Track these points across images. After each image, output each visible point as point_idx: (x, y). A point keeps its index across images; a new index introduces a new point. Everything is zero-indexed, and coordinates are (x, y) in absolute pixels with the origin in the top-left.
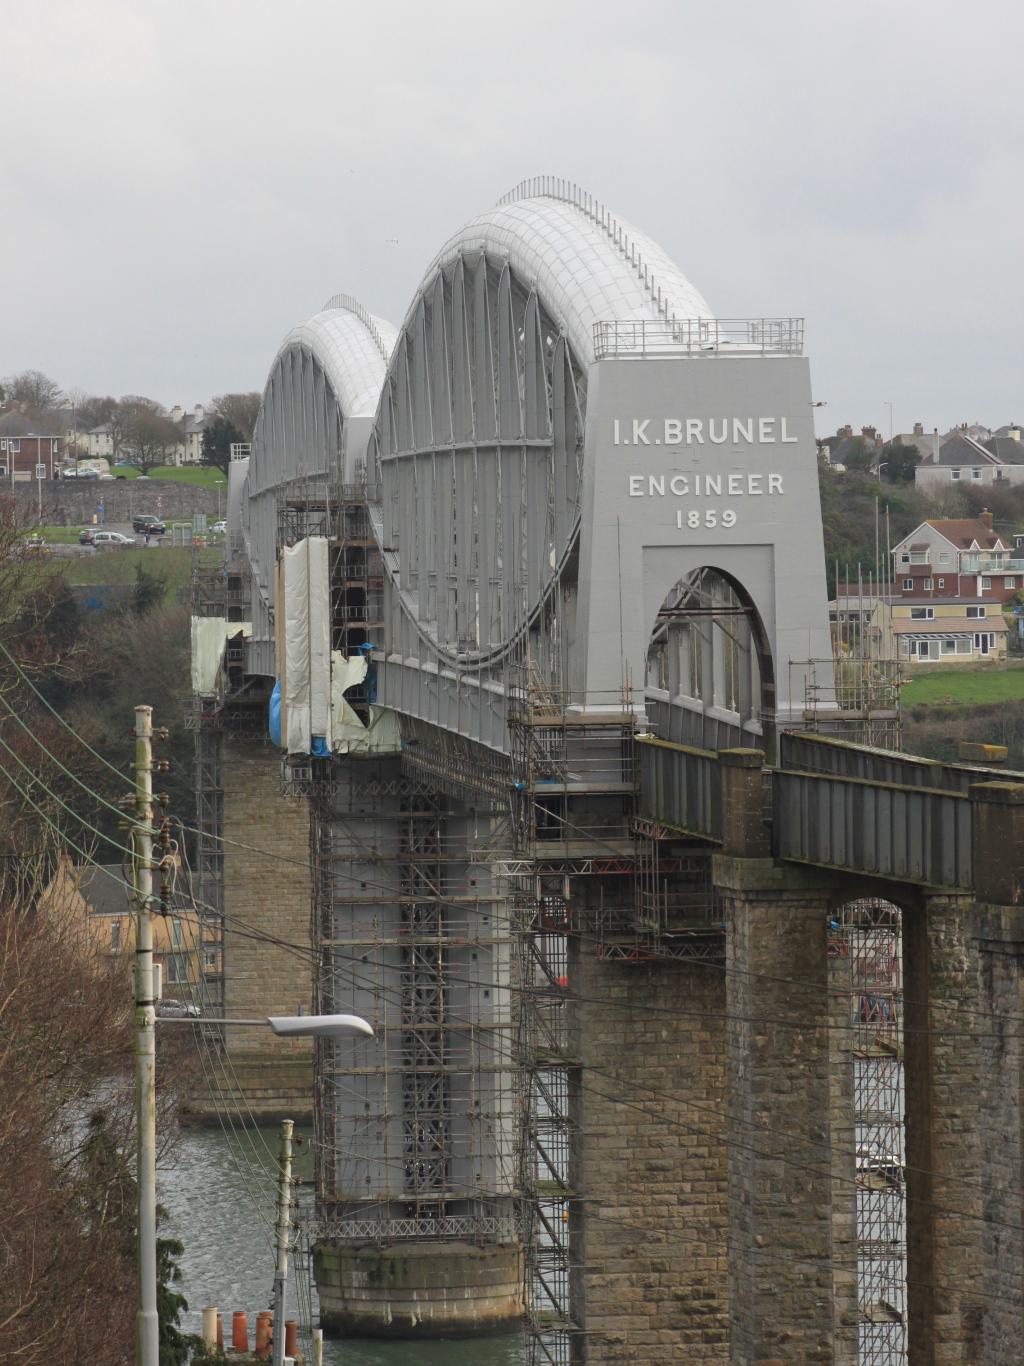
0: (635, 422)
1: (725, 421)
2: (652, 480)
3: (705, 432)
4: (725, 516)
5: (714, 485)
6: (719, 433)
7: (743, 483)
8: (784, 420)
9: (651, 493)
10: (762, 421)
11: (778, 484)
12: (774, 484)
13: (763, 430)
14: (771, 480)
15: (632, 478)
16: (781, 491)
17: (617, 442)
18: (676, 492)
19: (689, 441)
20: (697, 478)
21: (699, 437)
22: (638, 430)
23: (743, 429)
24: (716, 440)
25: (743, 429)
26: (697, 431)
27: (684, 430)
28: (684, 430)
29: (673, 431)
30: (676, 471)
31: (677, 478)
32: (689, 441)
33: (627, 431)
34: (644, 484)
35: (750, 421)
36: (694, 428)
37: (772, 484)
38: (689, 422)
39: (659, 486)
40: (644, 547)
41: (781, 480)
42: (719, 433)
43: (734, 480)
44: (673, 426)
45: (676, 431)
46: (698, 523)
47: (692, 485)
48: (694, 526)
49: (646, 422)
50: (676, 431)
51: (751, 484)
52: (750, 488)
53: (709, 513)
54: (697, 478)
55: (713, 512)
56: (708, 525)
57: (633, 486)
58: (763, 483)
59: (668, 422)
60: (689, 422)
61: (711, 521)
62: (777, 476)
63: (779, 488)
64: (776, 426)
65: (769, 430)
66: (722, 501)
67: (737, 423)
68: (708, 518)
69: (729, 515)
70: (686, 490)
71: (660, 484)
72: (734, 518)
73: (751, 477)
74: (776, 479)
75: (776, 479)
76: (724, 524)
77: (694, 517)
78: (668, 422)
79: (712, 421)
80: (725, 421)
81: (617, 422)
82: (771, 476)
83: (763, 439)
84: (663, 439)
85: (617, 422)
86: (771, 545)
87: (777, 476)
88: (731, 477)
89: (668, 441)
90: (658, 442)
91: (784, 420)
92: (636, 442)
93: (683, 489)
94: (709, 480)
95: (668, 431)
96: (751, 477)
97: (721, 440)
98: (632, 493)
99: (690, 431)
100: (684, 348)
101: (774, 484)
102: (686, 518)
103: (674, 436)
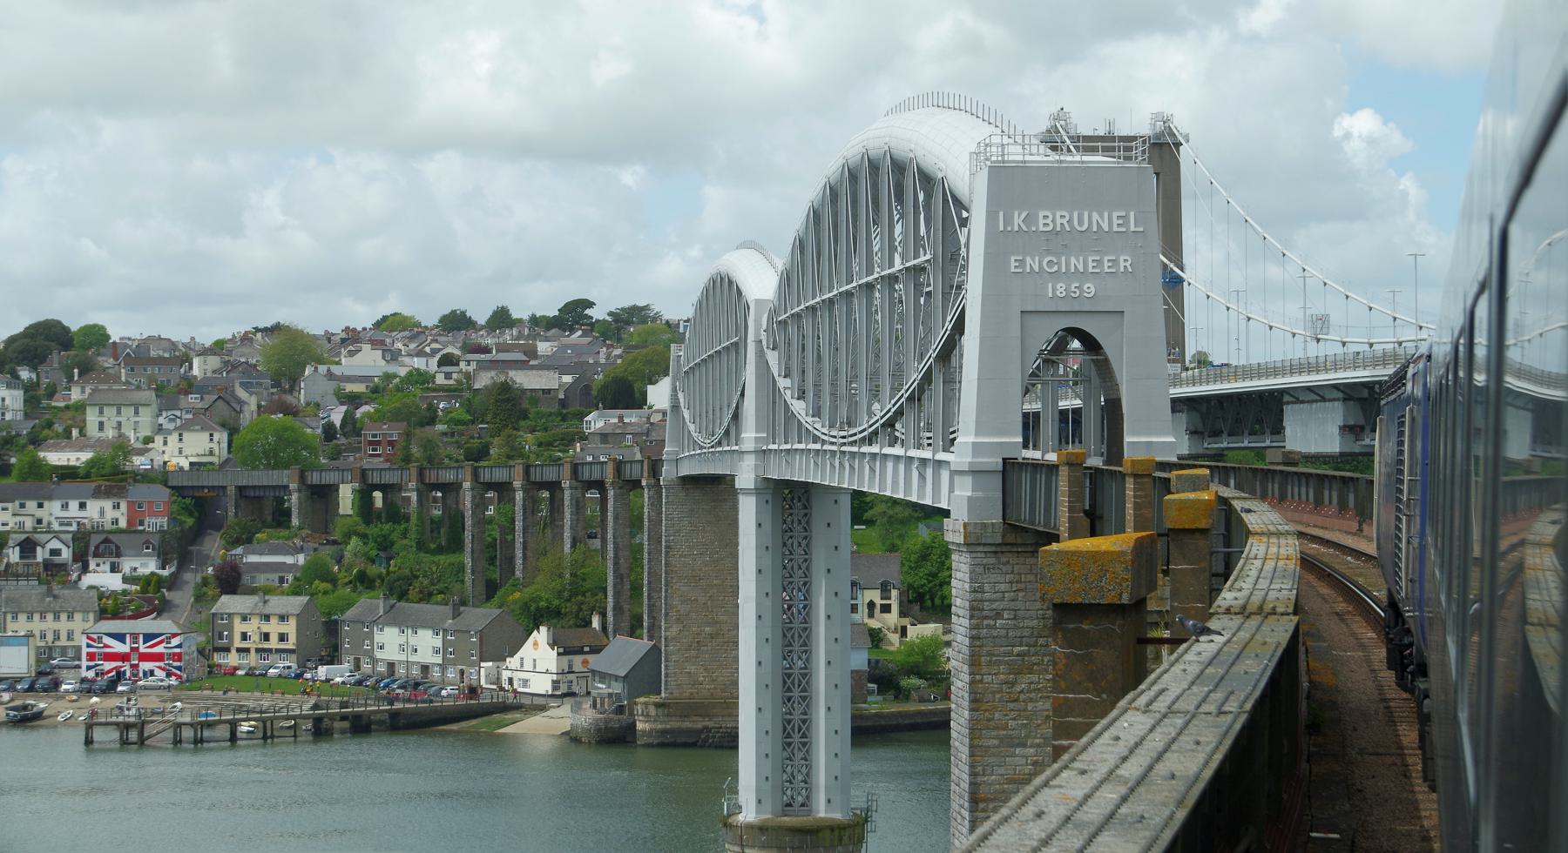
0: (1016, 214)
1: (1086, 214)
2: (1029, 260)
6: (1081, 223)
7: (1099, 263)
8: (1132, 214)
10: (1115, 215)
11: (1128, 264)
12: (1125, 264)
13: (1116, 222)
14: (1122, 261)
17: (1002, 228)
18: (1047, 269)
19: (1059, 229)
20: (1063, 259)
21: (1066, 225)
22: (1018, 219)
23: (1102, 220)
24: (1079, 229)
25: (1102, 220)
26: (1065, 221)
27: (1054, 221)
28: (1054, 221)
29: (1046, 220)
30: (1049, 252)
34: (1022, 262)
35: (1106, 214)
36: (1061, 218)
37: (1122, 264)
38: (1058, 214)
39: (1032, 263)
41: (1129, 262)
42: (1081, 223)
44: (1046, 217)
45: (1049, 221)
48: (1062, 295)
49: (1024, 215)
50: (1049, 221)
51: (1106, 264)
52: (1106, 268)
53: (1073, 286)
54: (1063, 259)
56: (1073, 295)
57: (1013, 264)
58: (1115, 262)
59: (1041, 214)
60: (1058, 214)
63: (1129, 267)
66: (1083, 275)
67: (1095, 216)
68: (1073, 289)
69: (1089, 288)
70: (1056, 268)
71: (1035, 263)
72: (1093, 289)
73: (1106, 259)
74: (1126, 260)
75: (1126, 260)
76: (1086, 294)
78: (1041, 214)
79: (1076, 215)
80: (1086, 214)
81: (1001, 214)
83: (1115, 229)
84: (1037, 228)
85: (1001, 214)
86: (1123, 312)
88: (1090, 259)
89: (1042, 228)
90: (1034, 229)
91: (1132, 214)
92: (1016, 228)
94: (1073, 260)
95: (1041, 221)
96: (1106, 259)
97: (1084, 228)
99: (1059, 221)
101: (1125, 264)
102: (1054, 290)
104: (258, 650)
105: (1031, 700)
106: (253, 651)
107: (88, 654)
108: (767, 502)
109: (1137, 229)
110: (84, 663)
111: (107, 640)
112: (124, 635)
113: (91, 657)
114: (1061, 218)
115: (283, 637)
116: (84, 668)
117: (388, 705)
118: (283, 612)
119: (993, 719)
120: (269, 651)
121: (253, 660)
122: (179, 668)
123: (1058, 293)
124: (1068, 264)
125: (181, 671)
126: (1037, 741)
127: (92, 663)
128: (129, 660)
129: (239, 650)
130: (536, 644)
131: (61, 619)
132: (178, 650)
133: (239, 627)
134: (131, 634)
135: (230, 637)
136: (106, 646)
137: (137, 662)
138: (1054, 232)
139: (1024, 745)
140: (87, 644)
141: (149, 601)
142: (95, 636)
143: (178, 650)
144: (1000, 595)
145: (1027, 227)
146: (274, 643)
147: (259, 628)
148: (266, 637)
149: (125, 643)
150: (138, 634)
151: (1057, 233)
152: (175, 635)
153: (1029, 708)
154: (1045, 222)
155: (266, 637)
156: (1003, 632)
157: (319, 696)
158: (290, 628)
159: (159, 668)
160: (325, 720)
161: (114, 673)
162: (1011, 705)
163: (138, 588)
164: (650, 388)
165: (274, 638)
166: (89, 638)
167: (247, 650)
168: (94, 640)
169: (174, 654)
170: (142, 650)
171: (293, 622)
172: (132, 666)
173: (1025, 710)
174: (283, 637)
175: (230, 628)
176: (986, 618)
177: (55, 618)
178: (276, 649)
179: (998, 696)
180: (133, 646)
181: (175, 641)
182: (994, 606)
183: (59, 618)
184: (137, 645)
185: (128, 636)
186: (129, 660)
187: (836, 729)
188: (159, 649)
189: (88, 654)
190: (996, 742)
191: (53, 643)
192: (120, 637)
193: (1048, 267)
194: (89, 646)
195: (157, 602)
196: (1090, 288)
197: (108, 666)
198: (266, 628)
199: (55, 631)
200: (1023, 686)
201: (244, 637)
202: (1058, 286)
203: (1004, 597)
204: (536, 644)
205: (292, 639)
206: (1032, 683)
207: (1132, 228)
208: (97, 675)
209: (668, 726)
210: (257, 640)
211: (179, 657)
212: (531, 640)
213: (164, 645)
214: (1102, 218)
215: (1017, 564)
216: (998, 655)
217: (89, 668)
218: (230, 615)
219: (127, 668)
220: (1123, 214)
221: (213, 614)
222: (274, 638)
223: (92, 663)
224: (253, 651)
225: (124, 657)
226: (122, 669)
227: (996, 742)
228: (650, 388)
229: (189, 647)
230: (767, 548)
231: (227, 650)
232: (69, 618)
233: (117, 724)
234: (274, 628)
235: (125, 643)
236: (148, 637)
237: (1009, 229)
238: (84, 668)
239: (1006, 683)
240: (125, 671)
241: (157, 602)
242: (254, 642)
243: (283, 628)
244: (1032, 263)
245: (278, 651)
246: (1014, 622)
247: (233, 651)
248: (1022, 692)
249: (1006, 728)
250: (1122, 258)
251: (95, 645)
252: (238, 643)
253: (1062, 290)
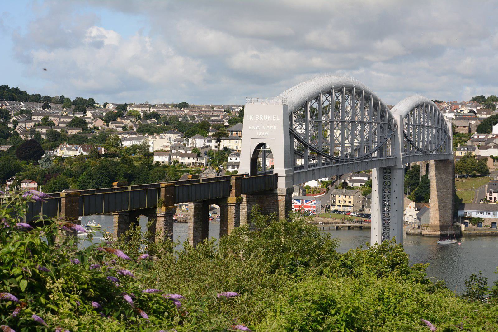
3: (263, 118)
6: (265, 118)
13: (273, 118)
22: (251, 118)
23: (270, 118)
25: (270, 118)
33: (249, 117)
34: (252, 127)
36: (261, 117)
39: (254, 128)
42: (265, 118)
47: (260, 127)
51: (271, 128)
72: (267, 133)
77: (260, 133)
78: (256, 116)
95: (256, 118)
99: (260, 117)
103: (257, 118)
104: (343, 206)
106: (341, 206)
114: (261, 117)
118: (350, 195)
120: (346, 206)
124: (262, 127)
128: (301, 207)
129: (338, 206)
130: (410, 207)
132: (314, 205)
136: (295, 203)
143: (314, 205)
146: (347, 204)
155: (345, 202)
157: (345, 220)
164: (494, 127)
165: (347, 202)
167: (340, 206)
169: (313, 206)
170: (305, 204)
174: (349, 202)
181: (314, 202)
188: (309, 205)
192: (299, 201)
198: (345, 199)
201: (340, 202)
204: (410, 207)
205: (352, 203)
209: (430, 233)
210: (343, 203)
212: (409, 206)
213: (311, 203)
214: (270, 117)
222: (347, 202)
224: (341, 206)
225: (299, 207)
228: (494, 127)
231: (335, 205)
234: (347, 199)
244: (254, 128)
245: (348, 206)
247: (336, 205)
252: (337, 203)
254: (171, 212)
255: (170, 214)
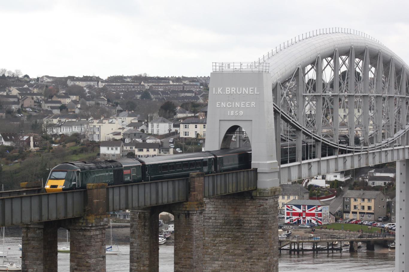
2: (222, 103)
4: (240, 113)
5: (238, 105)
6: (239, 91)
7: (245, 104)
8: (256, 88)
9: (222, 107)
10: (250, 88)
11: (254, 105)
12: (253, 105)
13: (250, 91)
15: (217, 103)
16: (254, 107)
17: (214, 93)
19: (232, 93)
20: (233, 103)
22: (219, 90)
23: (245, 91)
25: (245, 91)
26: (234, 91)
27: (231, 91)
28: (231, 91)
29: (228, 91)
31: (229, 103)
32: (232, 93)
33: (217, 90)
34: (220, 104)
35: (247, 88)
36: (233, 90)
37: (252, 105)
40: (220, 120)
42: (239, 91)
43: (243, 104)
44: (228, 89)
45: (229, 91)
46: (233, 114)
47: (232, 105)
49: (222, 88)
51: (247, 105)
52: (247, 106)
54: (233, 103)
55: (237, 112)
56: (236, 115)
57: (217, 105)
58: (250, 104)
60: (232, 88)
61: (236, 114)
62: (254, 103)
63: (254, 106)
64: (253, 89)
65: (252, 91)
66: (239, 109)
67: (244, 89)
68: (236, 113)
69: (241, 112)
72: (242, 113)
73: (247, 103)
76: (240, 115)
78: (227, 88)
81: (214, 88)
82: (252, 103)
83: (250, 93)
85: (214, 88)
86: (252, 120)
87: (254, 103)
89: (227, 93)
90: (224, 93)
92: (219, 93)
93: (229, 106)
94: (236, 103)
95: (227, 91)
96: (247, 103)
98: (217, 107)
99: (232, 91)
100: (251, 70)
101: (253, 105)
102: (230, 113)
103: (228, 92)
104: (360, 213)
105: (220, 246)
106: (358, 213)
107: (287, 212)
108: (404, 165)
109: (257, 93)
110: (286, 216)
111: (294, 207)
112: (300, 206)
113: (288, 214)
114: (233, 90)
115: (369, 208)
116: (286, 218)
117: (383, 237)
118: (369, 197)
119: (208, 252)
120: (364, 213)
121: (358, 217)
122: (321, 219)
123: (231, 114)
124: (235, 104)
125: (321, 221)
126: (222, 259)
127: (288, 217)
128: (302, 216)
129: (353, 213)
131: (285, 198)
132: (320, 212)
133: (353, 203)
134: (303, 205)
135: (350, 207)
137: (305, 217)
138: (231, 94)
139: (218, 260)
140: (287, 209)
141: (333, 191)
142: (290, 206)
143: (320, 212)
144: (210, 212)
145: (222, 92)
146: (366, 210)
147: (360, 204)
148: (363, 207)
149: (300, 209)
150: (306, 205)
151: (232, 95)
152: (319, 206)
153: (219, 249)
154: (228, 91)
155: (363, 207)
156: (211, 224)
158: (372, 204)
159: (314, 219)
160: (354, 242)
161: (296, 221)
162: (214, 247)
163: (329, 185)
165: (366, 208)
166: (287, 206)
167: (356, 213)
168: (289, 207)
169: (319, 214)
170: (307, 212)
171: (373, 201)
172: (304, 218)
173: (218, 249)
174: (369, 208)
175: (349, 203)
176: (206, 219)
177: (282, 198)
178: (367, 213)
179: (210, 244)
180: (303, 210)
181: (319, 209)
182: (209, 216)
183: (284, 198)
184: (305, 210)
185: (302, 206)
186: (302, 216)
187: (403, 252)
188: (313, 212)
189: (287, 212)
190: (209, 259)
191: (282, 208)
192: (299, 207)
193: (228, 106)
194: (287, 210)
195: (335, 192)
196: (241, 113)
197: (294, 218)
198: (363, 204)
199: (282, 203)
200: (218, 241)
201: (355, 207)
202: (231, 112)
203: (212, 212)
206: (220, 240)
207: (256, 93)
208: (290, 221)
211: (320, 215)
213: (315, 210)
214: (246, 89)
215: (216, 202)
216: (210, 231)
217: (287, 218)
218: (350, 198)
219: (301, 218)
220: (253, 88)
221: (344, 198)
222: (366, 208)
223: (288, 217)
224: (358, 213)
225: (300, 214)
226: (300, 219)
227: (209, 259)
229: (326, 211)
230: (404, 183)
231: (349, 212)
232: (288, 198)
233: (311, 242)
234: (366, 204)
235: (300, 209)
236: (309, 207)
237: (216, 93)
238: (286, 218)
239: (212, 240)
240: (301, 220)
241: (335, 192)
242: (359, 209)
243: (370, 204)
245: (368, 213)
246: (215, 221)
247: (351, 213)
248: (217, 243)
249: (212, 254)
250: (252, 103)
251: (290, 209)
252: (352, 209)
253: (232, 113)
254: (102, 223)
255: (101, 226)
